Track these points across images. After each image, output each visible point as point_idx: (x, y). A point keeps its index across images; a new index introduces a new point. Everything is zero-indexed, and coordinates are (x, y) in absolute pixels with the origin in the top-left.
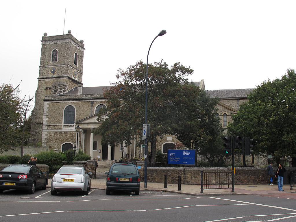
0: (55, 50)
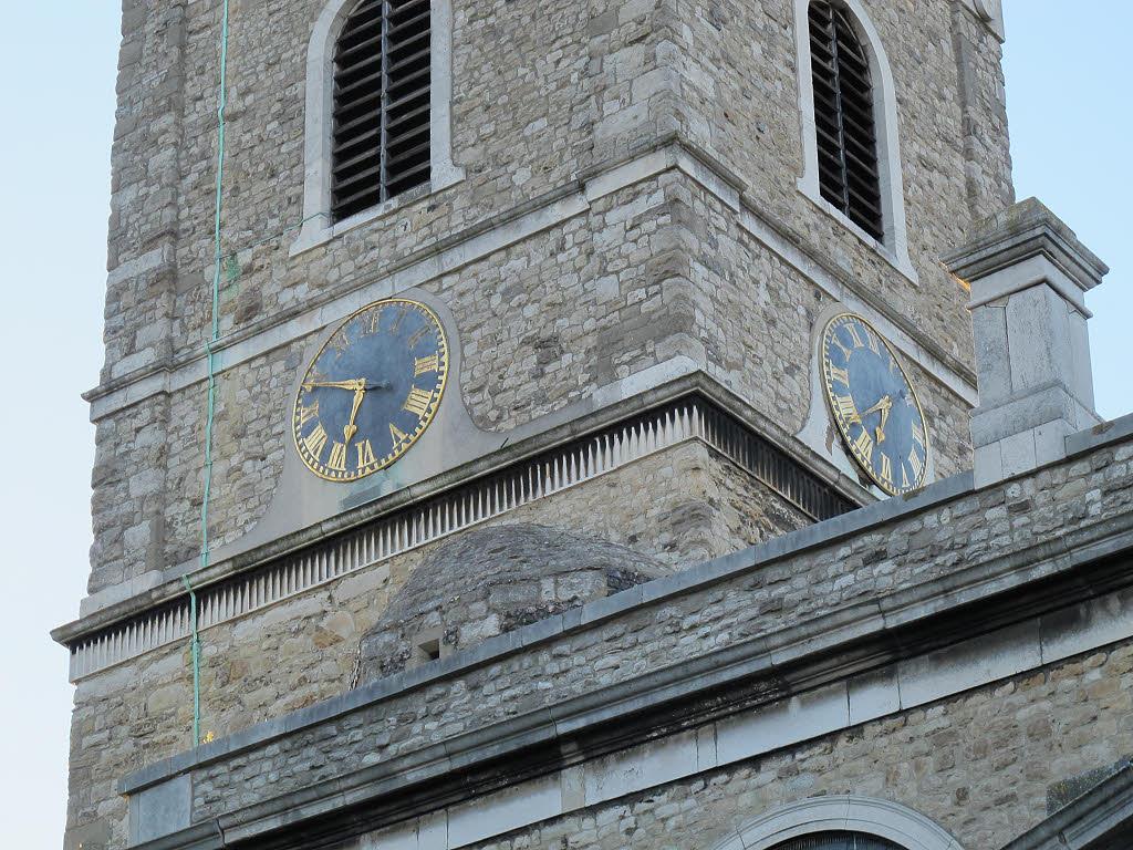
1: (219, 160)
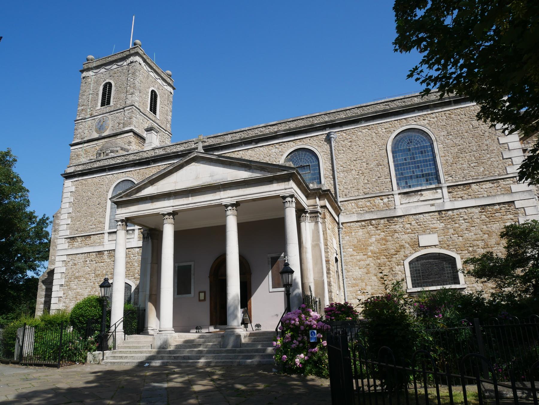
1: (90, 98)
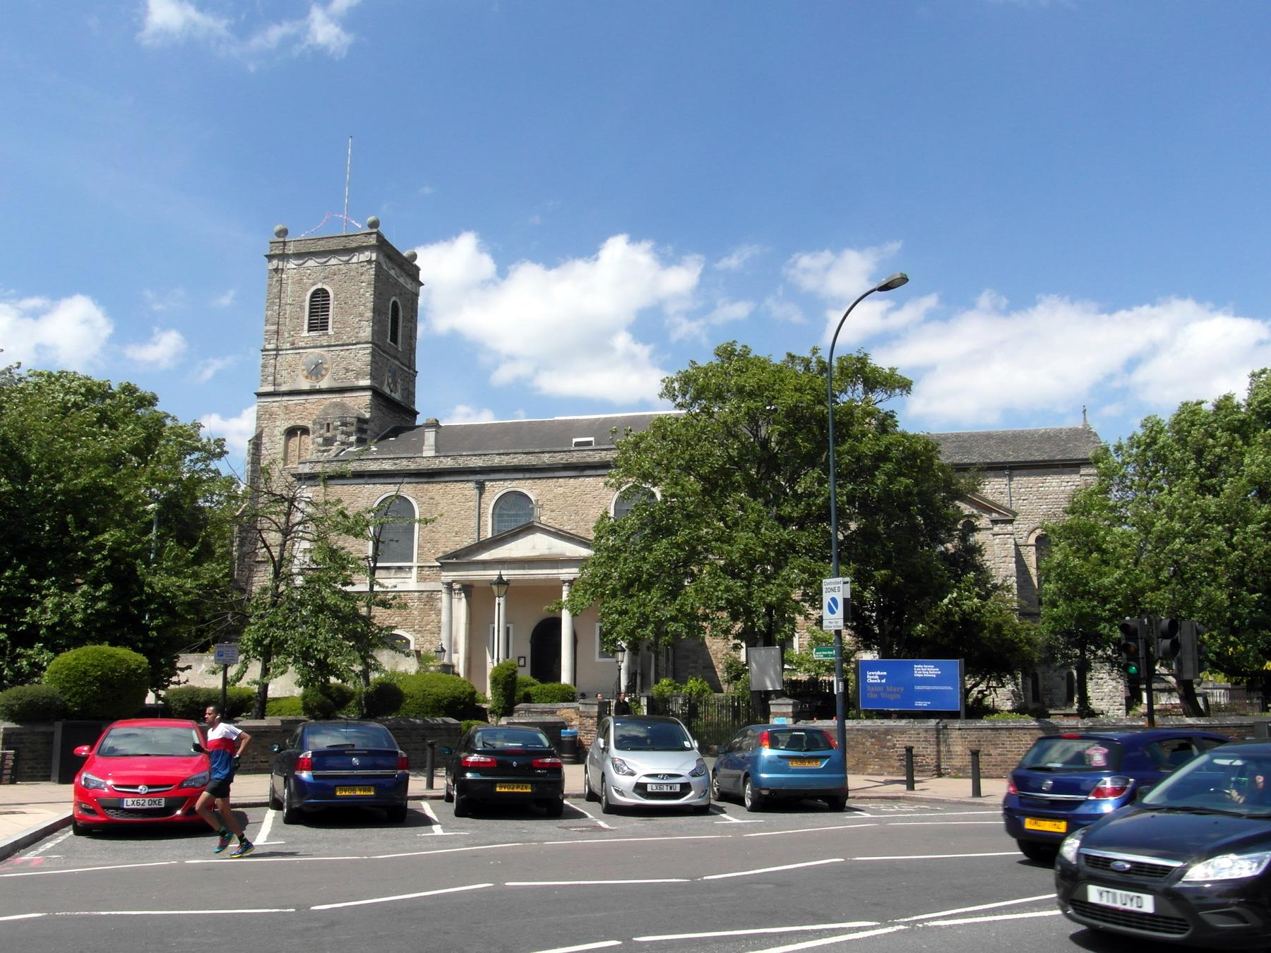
0: (318, 290)
1: (288, 312)
